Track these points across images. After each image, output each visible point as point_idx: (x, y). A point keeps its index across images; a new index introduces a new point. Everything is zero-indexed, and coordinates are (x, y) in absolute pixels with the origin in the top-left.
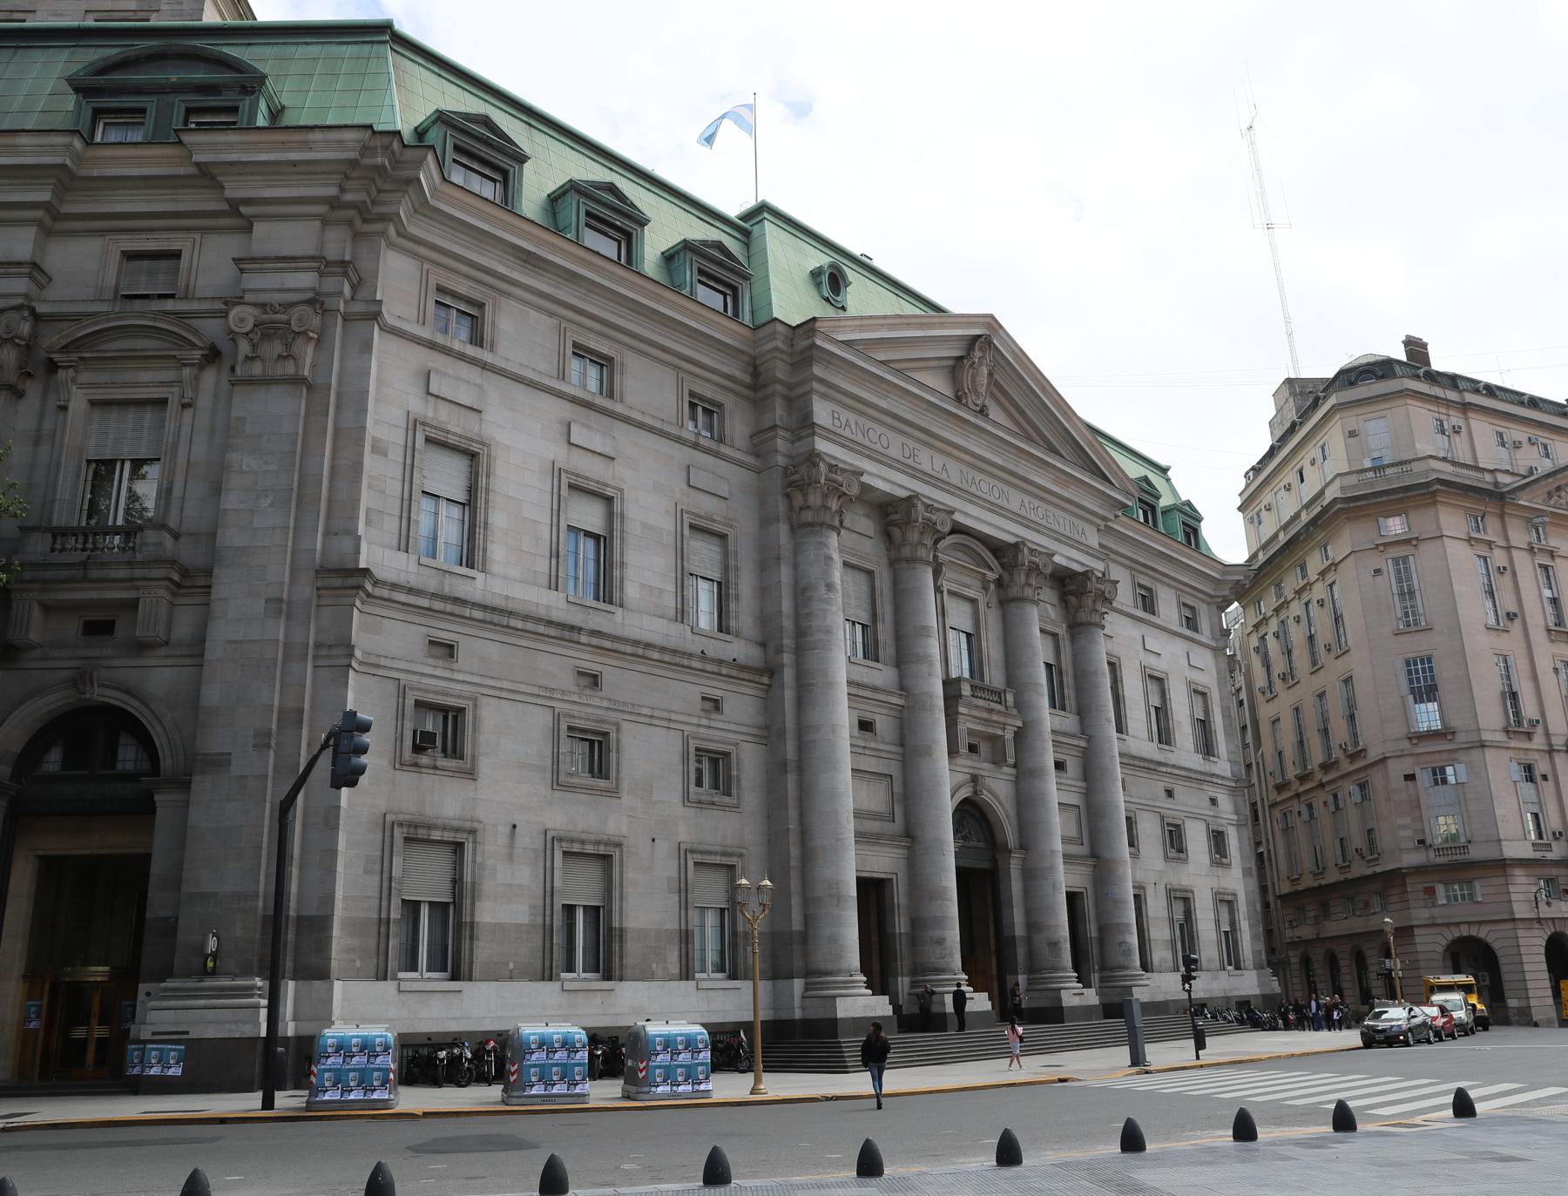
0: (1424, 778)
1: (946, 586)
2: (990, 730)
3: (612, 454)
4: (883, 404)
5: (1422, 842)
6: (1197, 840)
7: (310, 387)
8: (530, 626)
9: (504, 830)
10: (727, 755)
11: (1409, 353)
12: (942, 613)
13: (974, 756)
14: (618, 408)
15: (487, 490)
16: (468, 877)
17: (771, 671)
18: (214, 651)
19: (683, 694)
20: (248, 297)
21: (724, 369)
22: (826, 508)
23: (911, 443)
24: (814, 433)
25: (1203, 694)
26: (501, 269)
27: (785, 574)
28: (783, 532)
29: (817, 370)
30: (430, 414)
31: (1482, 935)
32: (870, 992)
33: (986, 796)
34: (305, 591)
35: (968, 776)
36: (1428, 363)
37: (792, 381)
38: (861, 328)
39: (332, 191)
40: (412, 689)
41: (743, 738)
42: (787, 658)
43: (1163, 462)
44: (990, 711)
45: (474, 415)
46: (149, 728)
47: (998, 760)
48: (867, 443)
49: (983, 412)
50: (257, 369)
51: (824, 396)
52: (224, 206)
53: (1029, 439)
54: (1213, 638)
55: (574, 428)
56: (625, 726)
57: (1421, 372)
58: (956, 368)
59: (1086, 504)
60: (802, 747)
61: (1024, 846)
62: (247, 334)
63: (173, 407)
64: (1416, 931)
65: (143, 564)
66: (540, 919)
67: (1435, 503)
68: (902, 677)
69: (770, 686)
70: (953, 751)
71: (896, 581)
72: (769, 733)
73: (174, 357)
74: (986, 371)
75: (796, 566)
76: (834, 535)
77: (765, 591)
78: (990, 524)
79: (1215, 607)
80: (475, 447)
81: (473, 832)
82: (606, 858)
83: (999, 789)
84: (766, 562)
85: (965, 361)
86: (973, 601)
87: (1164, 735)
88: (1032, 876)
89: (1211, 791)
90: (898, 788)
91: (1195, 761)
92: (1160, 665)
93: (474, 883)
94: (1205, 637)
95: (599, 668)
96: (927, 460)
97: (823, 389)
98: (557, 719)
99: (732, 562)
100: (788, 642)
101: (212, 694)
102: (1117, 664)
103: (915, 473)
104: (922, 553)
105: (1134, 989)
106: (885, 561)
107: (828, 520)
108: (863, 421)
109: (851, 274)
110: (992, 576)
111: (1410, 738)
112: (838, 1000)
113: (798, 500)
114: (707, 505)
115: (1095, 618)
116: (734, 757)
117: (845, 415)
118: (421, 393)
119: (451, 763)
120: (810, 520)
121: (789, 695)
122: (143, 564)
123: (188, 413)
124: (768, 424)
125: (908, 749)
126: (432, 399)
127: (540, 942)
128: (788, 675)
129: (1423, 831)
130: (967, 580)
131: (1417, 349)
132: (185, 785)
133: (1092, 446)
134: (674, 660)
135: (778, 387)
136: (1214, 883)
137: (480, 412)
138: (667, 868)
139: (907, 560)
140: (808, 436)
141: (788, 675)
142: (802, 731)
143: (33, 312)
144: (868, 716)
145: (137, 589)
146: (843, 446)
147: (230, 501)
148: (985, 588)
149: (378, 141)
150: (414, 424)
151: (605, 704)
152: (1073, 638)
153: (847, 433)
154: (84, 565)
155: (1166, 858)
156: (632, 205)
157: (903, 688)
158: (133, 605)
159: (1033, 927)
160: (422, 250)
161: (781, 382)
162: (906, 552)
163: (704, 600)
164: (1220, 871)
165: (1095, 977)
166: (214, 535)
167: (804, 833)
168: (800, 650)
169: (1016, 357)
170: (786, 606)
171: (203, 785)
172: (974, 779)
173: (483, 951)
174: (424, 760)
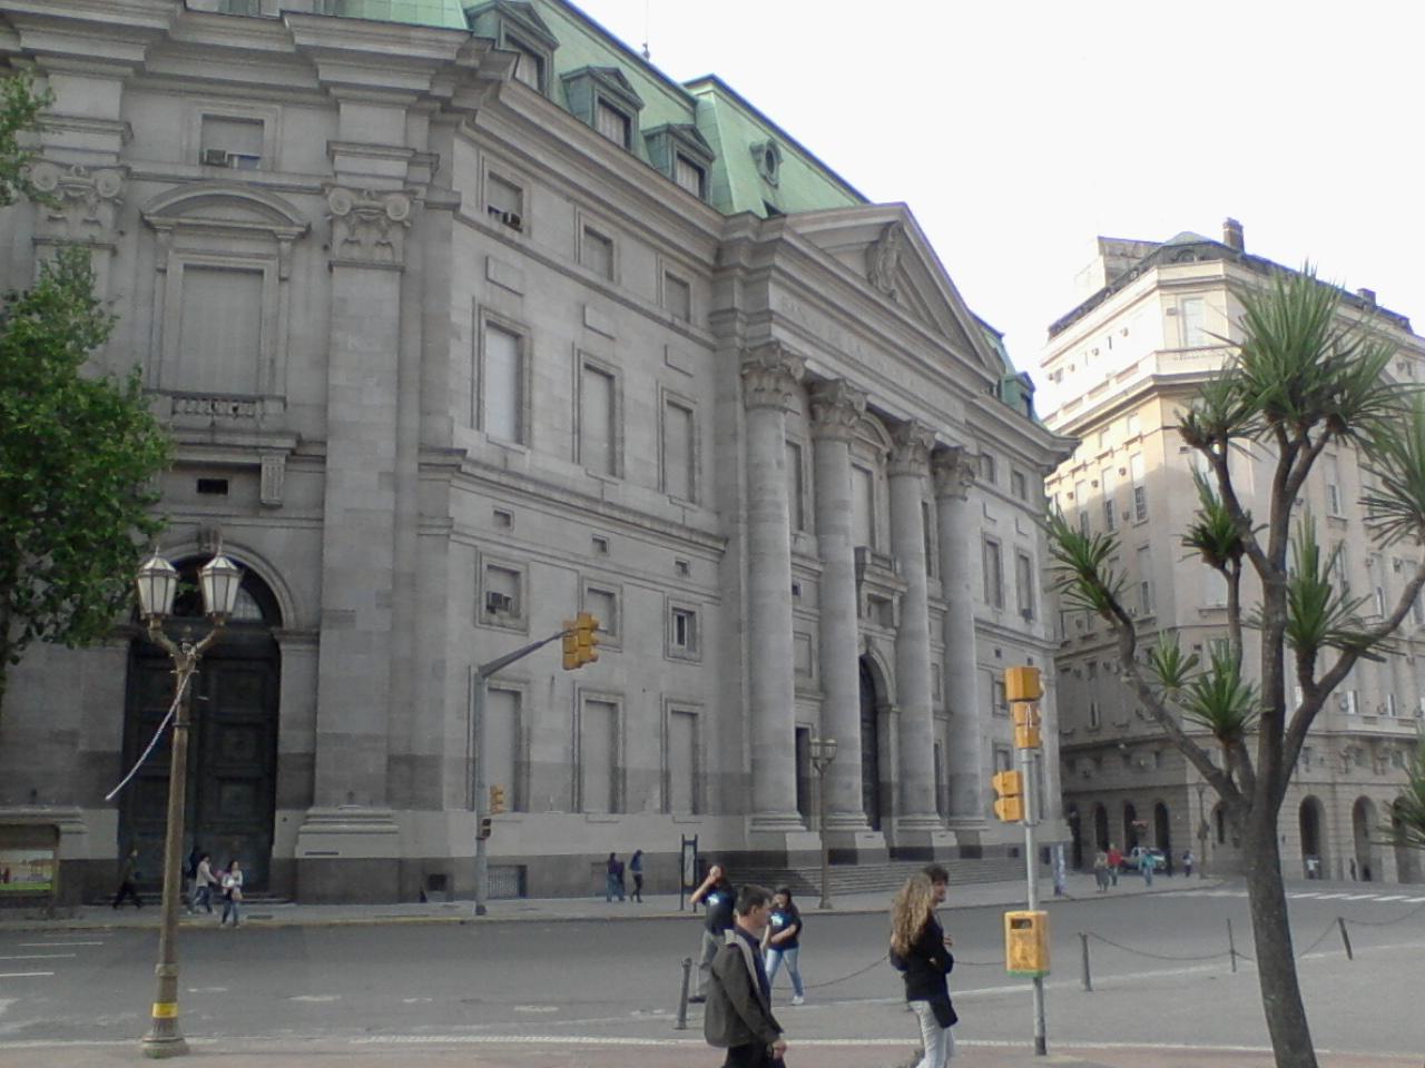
2: (882, 595)
3: (614, 335)
4: (822, 290)
8: (565, 498)
9: (548, 680)
10: (691, 614)
14: (619, 292)
15: (531, 372)
16: (524, 724)
17: (726, 541)
18: (333, 516)
19: (661, 558)
20: (342, 180)
21: (699, 254)
22: (777, 390)
24: (771, 320)
25: (1026, 559)
26: (540, 158)
28: (739, 407)
29: (778, 261)
30: (488, 298)
32: (804, 828)
33: (875, 656)
34: (410, 466)
36: (1242, 246)
37: (752, 267)
38: (814, 222)
39: (423, 85)
40: (488, 555)
41: (706, 599)
42: (742, 527)
44: (883, 577)
45: (517, 299)
46: (271, 584)
49: (891, 296)
50: (356, 253)
51: (778, 283)
52: (315, 85)
53: (919, 318)
55: (587, 310)
56: (626, 587)
57: (1238, 256)
58: (870, 251)
59: (961, 383)
60: (753, 610)
61: (901, 701)
62: (344, 217)
63: (270, 278)
65: (267, 434)
66: (570, 761)
68: (820, 546)
69: (724, 552)
71: (816, 457)
72: (721, 596)
73: (271, 231)
74: (895, 257)
75: (749, 444)
76: (782, 415)
78: (895, 406)
80: (520, 331)
81: (527, 682)
82: (516, 695)
83: (884, 650)
84: (718, 441)
85: (879, 246)
86: (868, 473)
87: (998, 600)
88: (902, 728)
89: (1029, 652)
90: (815, 646)
92: (996, 531)
93: (529, 730)
94: (1030, 504)
95: (606, 534)
96: (849, 343)
98: (581, 579)
100: (743, 513)
101: (333, 556)
103: (838, 355)
105: (982, 834)
109: (784, 151)
110: (885, 450)
111: (1200, 611)
112: (787, 835)
113: (754, 382)
114: (679, 382)
115: (960, 492)
116: (697, 615)
118: (482, 278)
119: (511, 622)
120: (763, 401)
121: (743, 562)
122: (267, 434)
123: (286, 286)
124: (727, 306)
125: (823, 616)
126: (489, 284)
127: (570, 779)
128: (743, 540)
130: (865, 453)
131: (1235, 230)
132: (315, 639)
133: (971, 329)
134: (663, 531)
135: (739, 272)
137: (521, 295)
138: (652, 716)
139: (829, 438)
140: (764, 321)
141: (743, 540)
142: (753, 594)
143: (128, 170)
145: (260, 455)
147: (339, 378)
148: (879, 461)
149: (475, 45)
150: (480, 309)
151: (613, 568)
152: (939, 506)
154: (213, 428)
156: (632, 90)
157: (821, 556)
158: (256, 470)
159: (904, 774)
160: (482, 139)
162: (828, 431)
163: (677, 472)
165: (816, 820)
166: (324, 408)
167: (754, 689)
168: (752, 521)
169: (920, 242)
171: (326, 637)
173: (537, 786)
174: (495, 619)
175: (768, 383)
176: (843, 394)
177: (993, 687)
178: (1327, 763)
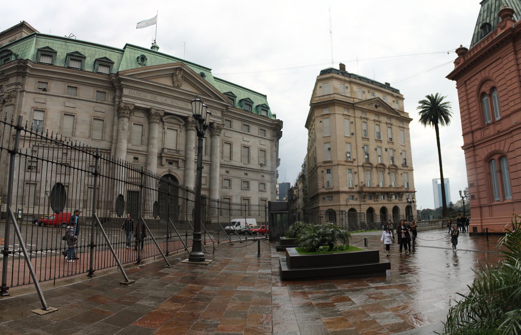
0: (325, 172)
1: (166, 128)
5: (323, 187)
6: (254, 186)
7: (14, 105)
11: (340, 67)
12: (164, 133)
13: (171, 165)
23: (154, 95)
27: (115, 127)
28: (116, 118)
31: (332, 208)
33: (173, 174)
35: (168, 170)
43: (264, 94)
47: (178, 167)
48: (139, 97)
51: (126, 88)
54: (271, 138)
64: (320, 207)
67: (335, 105)
70: (161, 165)
77: (112, 131)
79: (272, 130)
83: (178, 173)
86: (177, 130)
91: (258, 167)
97: (126, 86)
99: (104, 125)
102: (232, 143)
104: (155, 121)
106: (147, 122)
107: (124, 115)
108: (138, 92)
114: (99, 114)
117: (133, 91)
129: (324, 184)
131: (342, 66)
136: (260, 196)
144: (137, 157)
146: (131, 98)
152: (211, 138)
153: (133, 95)
155: (242, 189)
157: (147, 151)
161: (117, 86)
164: (262, 193)
168: (116, 143)
170: (115, 134)
172: (169, 171)
175: (122, 111)
176: (153, 111)
177: (242, 182)
178: (358, 199)
